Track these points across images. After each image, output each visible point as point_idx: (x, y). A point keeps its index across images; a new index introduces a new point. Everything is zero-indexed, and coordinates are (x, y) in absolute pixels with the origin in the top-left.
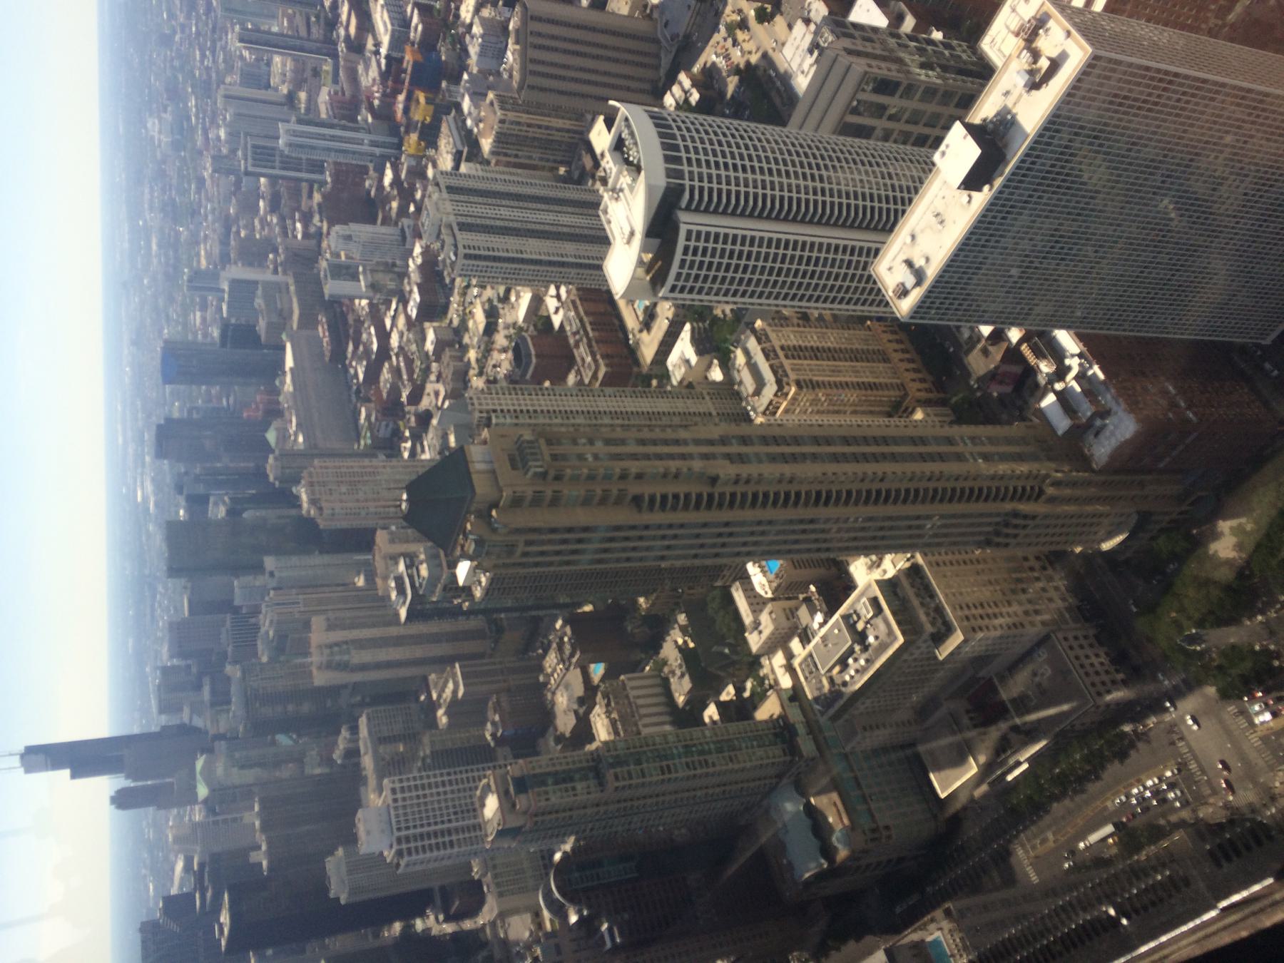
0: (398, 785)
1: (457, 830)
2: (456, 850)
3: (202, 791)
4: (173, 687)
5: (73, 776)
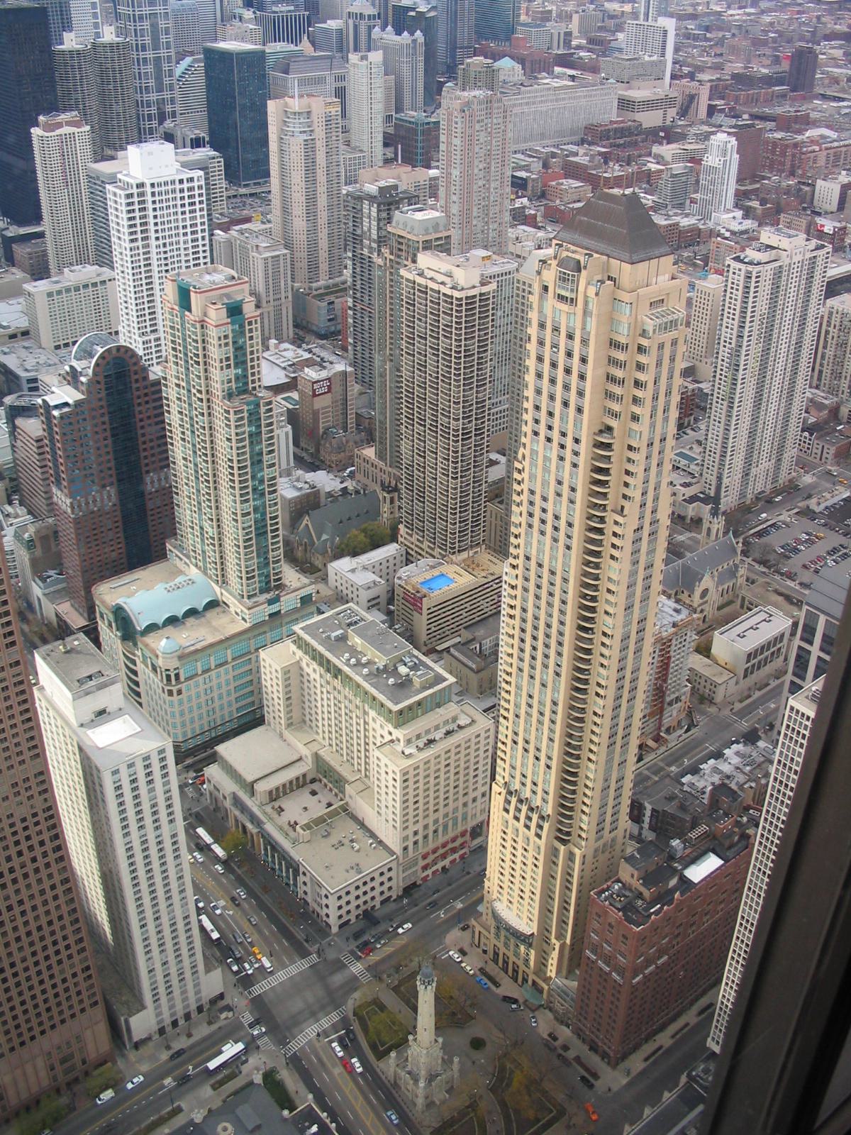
0: (196, 184)
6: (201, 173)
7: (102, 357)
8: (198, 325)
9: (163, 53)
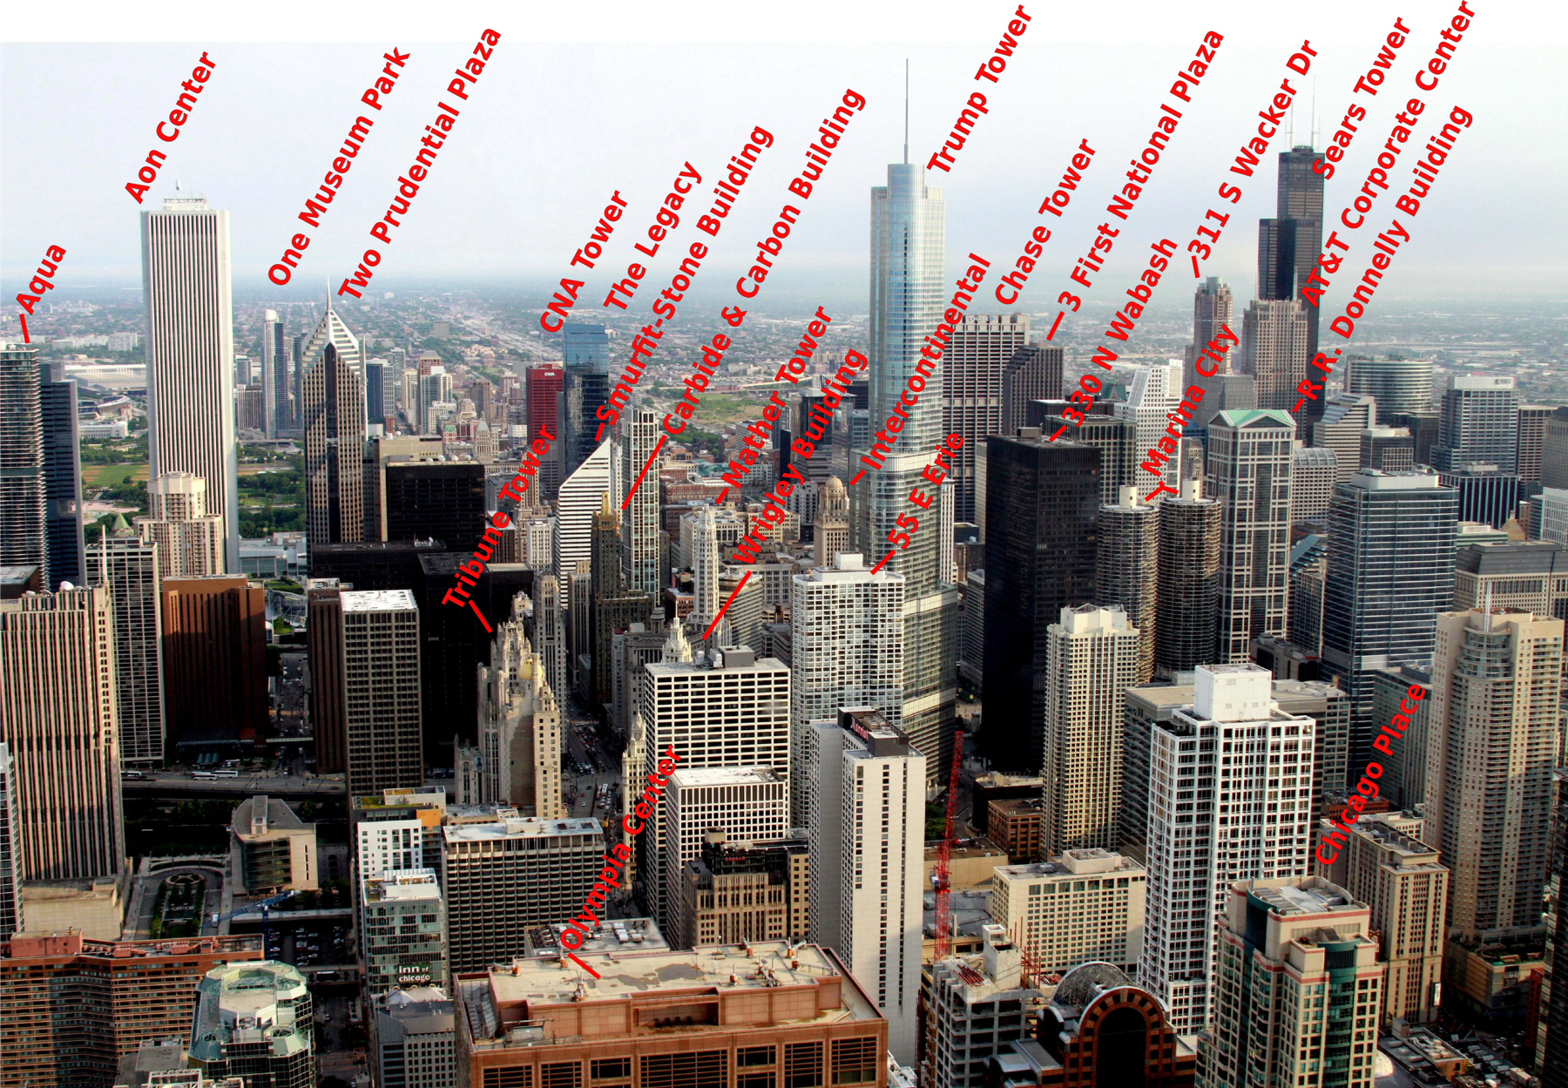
0: (1301, 738)
1: (1204, 831)
2: (1174, 826)
5: (1264, 223)
6: (1312, 722)
7: (1102, 1003)
8: (1273, 976)
9: (1271, 526)
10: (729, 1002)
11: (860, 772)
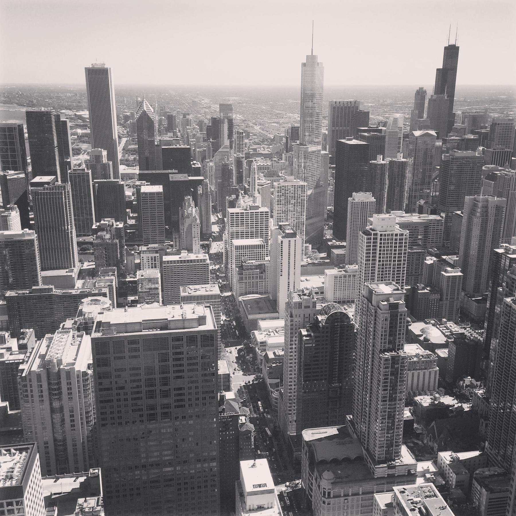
0: (404, 237)
3: (417, 133)
4: (475, 120)
5: (438, 70)
10: (171, 323)
11: (282, 242)
